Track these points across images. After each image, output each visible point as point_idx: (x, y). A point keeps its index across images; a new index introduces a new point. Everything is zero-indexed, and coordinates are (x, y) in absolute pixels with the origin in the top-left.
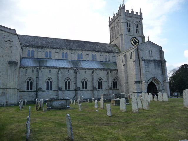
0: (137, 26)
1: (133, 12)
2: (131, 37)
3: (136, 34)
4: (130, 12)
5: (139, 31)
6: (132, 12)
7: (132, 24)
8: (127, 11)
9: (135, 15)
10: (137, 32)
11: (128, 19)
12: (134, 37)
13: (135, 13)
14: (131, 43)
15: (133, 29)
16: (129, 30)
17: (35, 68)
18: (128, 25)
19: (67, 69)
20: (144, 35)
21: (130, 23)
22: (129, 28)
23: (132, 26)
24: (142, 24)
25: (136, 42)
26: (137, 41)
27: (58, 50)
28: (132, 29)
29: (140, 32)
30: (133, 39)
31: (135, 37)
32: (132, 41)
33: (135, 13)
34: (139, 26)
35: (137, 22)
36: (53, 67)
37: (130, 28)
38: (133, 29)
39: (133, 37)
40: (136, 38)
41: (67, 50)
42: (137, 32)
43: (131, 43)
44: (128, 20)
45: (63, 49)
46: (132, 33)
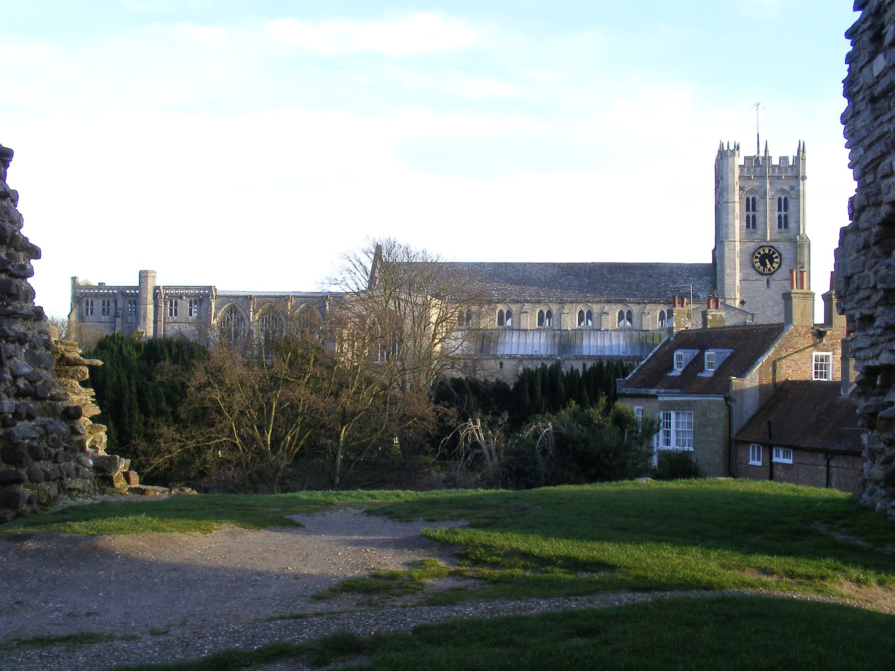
0: (783, 204)
2: (752, 246)
12: (764, 244)
13: (775, 161)
14: (754, 267)
17: (470, 359)
19: (540, 359)
21: (757, 198)
22: (751, 214)
23: (760, 207)
26: (777, 257)
27: (527, 306)
28: (760, 220)
29: (792, 225)
31: (770, 244)
33: (775, 161)
34: (791, 204)
35: (783, 191)
36: (508, 355)
37: (757, 214)
40: (772, 247)
41: (551, 305)
42: (783, 222)
43: (754, 267)
45: (539, 302)
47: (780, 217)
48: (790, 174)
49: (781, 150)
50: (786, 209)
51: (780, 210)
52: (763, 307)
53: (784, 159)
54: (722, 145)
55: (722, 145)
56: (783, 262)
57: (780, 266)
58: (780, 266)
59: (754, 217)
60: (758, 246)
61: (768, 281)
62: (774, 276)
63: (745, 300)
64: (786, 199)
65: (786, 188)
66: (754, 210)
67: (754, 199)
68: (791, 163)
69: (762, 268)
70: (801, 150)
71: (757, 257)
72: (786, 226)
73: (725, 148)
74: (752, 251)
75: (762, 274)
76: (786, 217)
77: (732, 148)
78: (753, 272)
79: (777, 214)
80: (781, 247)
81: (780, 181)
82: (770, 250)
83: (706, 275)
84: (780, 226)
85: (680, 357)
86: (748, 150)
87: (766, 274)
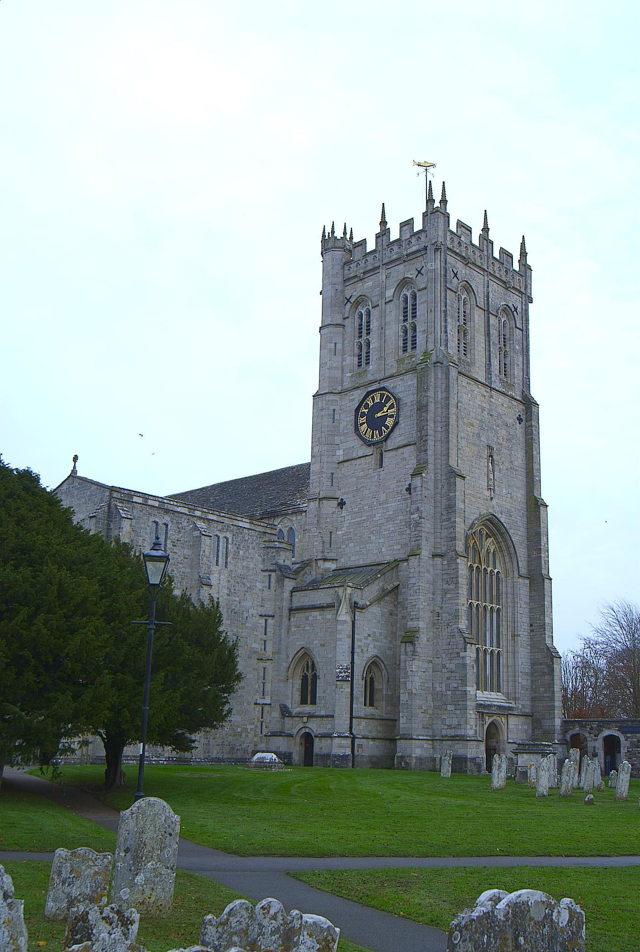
4: (371, 246)
6: (384, 232)
35: (404, 283)
39: (368, 394)
40: (384, 389)
52: (371, 506)
56: (401, 413)
57: (396, 424)
58: (396, 424)
62: (390, 444)
65: (411, 274)
78: (359, 442)
82: (382, 396)
87: (374, 444)
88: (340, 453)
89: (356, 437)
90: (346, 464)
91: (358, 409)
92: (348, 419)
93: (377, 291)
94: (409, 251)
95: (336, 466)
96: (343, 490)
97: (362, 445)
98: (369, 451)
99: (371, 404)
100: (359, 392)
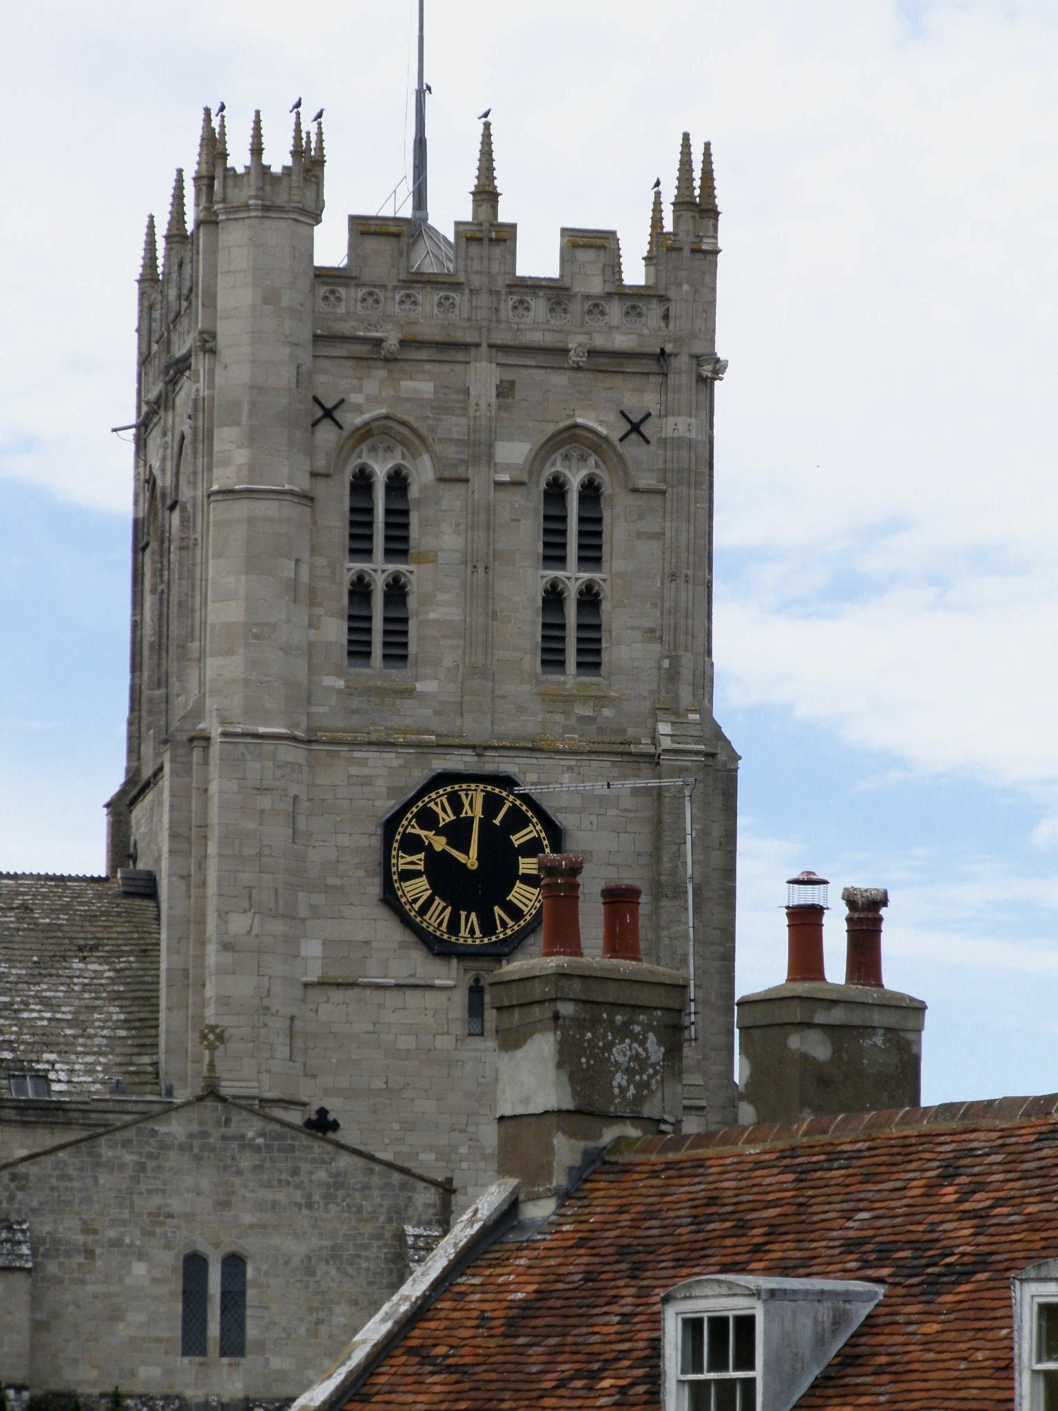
0: (572, 522)
1: (505, 237)
2: (384, 779)
3: (520, 700)
5: (613, 616)
7: (453, 498)
8: (362, 228)
9: (539, 307)
10: (572, 633)
11: (367, 396)
13: (537, 258)
14: (390, 899)
15: (473, 575)
16: (378, 626)
18: (379, 517)
20: (730, 706)
21: (422, 473)
22: (379, 570)
23: (440, 530)
24: (693, 474)
25: (512, 876)
28: (437, 607)
29: (626, 646)
30: (427, 819)
32: (403, 861)
33: (537, 258)
35: (572, 438)
37: (416, 575)
38: (473, 575)
40: (507, 782)
42: (572, 633)
44: (365, 433)
46: (433, 681)
47: (553, 598)
48: (621, 341)
49: (576, 189)
50: (591, 555)
51: (554, 555)
53: (589, 245)
54: (214, 146)
55: (214, 146)
59: (397, 591)
60: (420, 776)
61: (476, 991)
63: (336, 1108)
64: (591, 492)
65: (599, 420)
66: (398, 547)
67: (398, 483)
68: (634, 273)
69: (438, 917)
70: (695, 209)
71: (412, 845)
72: (591, 659)
73: (238, 159)
74: (389, 806)
75: (438, 948)
76: (590, 599)
77: (278, 157)
78: (388, 932)
79: (537, 578)
80: (558, 785)
81: (560, 380)
83: (85, 951)
84: (552, 658)
85: (726, 1339)
86: (360, 185)
88: (312, 949)
89: (383, 913)
90: (337, 995)
91: (391, 824)
92: (344, 840)
93: (456, 425)
94: (600, 342)
95: (299, 992)
96: (326, 1081)
97: (402, 945)
98: (446, 974)
99: (446, 817)
100: (390, 758)
